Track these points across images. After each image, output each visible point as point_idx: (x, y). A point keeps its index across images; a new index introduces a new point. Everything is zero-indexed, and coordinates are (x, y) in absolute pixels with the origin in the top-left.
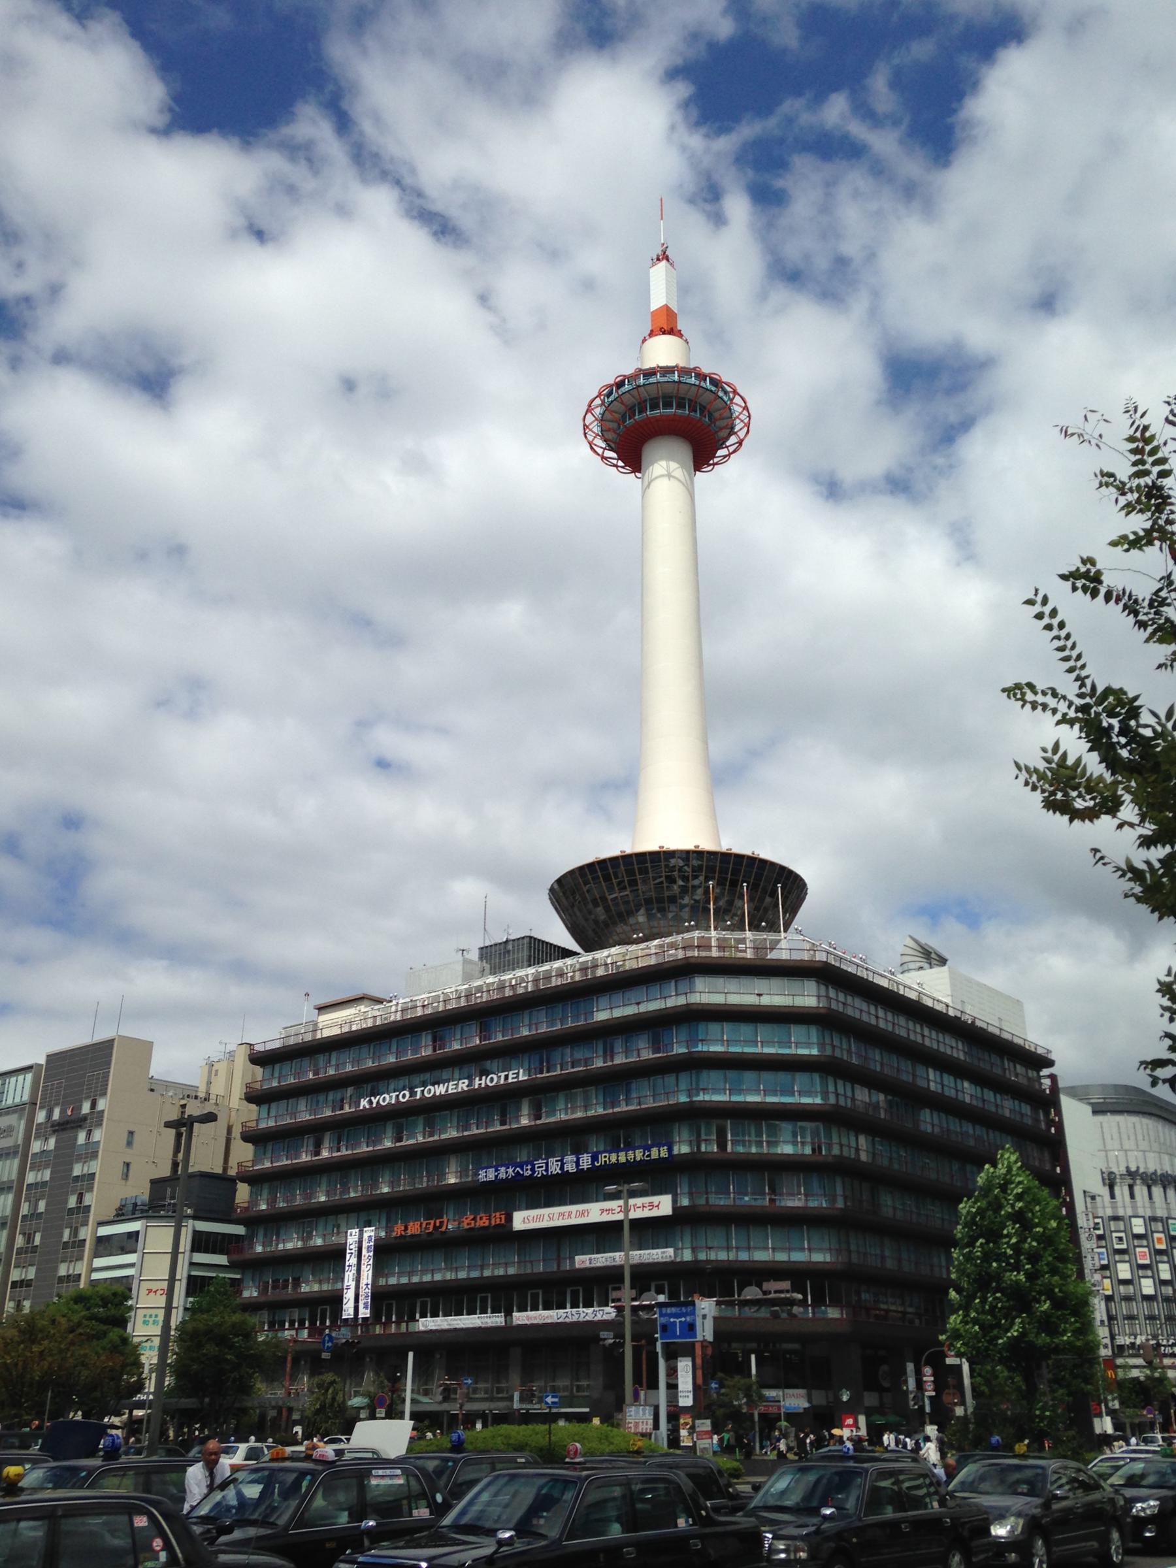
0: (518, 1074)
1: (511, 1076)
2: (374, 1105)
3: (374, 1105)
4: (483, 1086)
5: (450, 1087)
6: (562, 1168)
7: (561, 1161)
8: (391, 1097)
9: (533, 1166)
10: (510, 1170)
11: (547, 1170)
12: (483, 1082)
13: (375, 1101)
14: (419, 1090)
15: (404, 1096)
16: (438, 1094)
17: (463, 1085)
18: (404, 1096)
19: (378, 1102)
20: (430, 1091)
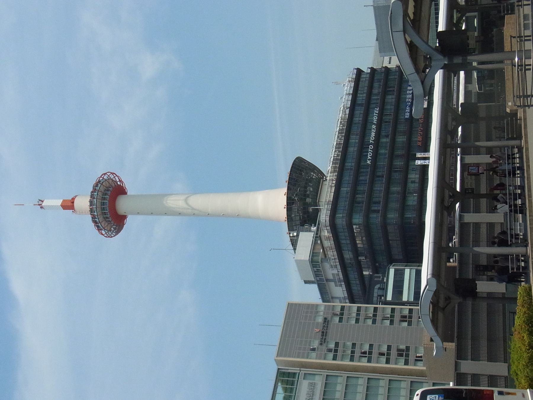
0: (376, 110)
1: (376, 112)
2: (371, 158)
3: (371, 158)
4: (376, 121)
5: (373, 131)
6: (410, 94)
7: (408, 94)
8: (370, 152)
9: (408, 102)
10: (407, 108)
11: (410, 98)
12: (375, 120)
13: (369, 158)
14: (371, 141)
15: (371, 147)
16: (374, 135)
17: (374, 127)
18: (371, 147)
19: (370, 156)
20: (372, 138)
